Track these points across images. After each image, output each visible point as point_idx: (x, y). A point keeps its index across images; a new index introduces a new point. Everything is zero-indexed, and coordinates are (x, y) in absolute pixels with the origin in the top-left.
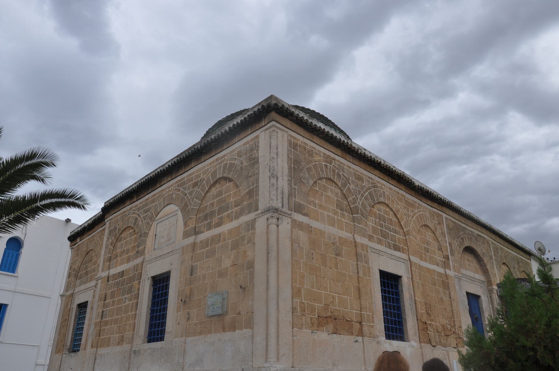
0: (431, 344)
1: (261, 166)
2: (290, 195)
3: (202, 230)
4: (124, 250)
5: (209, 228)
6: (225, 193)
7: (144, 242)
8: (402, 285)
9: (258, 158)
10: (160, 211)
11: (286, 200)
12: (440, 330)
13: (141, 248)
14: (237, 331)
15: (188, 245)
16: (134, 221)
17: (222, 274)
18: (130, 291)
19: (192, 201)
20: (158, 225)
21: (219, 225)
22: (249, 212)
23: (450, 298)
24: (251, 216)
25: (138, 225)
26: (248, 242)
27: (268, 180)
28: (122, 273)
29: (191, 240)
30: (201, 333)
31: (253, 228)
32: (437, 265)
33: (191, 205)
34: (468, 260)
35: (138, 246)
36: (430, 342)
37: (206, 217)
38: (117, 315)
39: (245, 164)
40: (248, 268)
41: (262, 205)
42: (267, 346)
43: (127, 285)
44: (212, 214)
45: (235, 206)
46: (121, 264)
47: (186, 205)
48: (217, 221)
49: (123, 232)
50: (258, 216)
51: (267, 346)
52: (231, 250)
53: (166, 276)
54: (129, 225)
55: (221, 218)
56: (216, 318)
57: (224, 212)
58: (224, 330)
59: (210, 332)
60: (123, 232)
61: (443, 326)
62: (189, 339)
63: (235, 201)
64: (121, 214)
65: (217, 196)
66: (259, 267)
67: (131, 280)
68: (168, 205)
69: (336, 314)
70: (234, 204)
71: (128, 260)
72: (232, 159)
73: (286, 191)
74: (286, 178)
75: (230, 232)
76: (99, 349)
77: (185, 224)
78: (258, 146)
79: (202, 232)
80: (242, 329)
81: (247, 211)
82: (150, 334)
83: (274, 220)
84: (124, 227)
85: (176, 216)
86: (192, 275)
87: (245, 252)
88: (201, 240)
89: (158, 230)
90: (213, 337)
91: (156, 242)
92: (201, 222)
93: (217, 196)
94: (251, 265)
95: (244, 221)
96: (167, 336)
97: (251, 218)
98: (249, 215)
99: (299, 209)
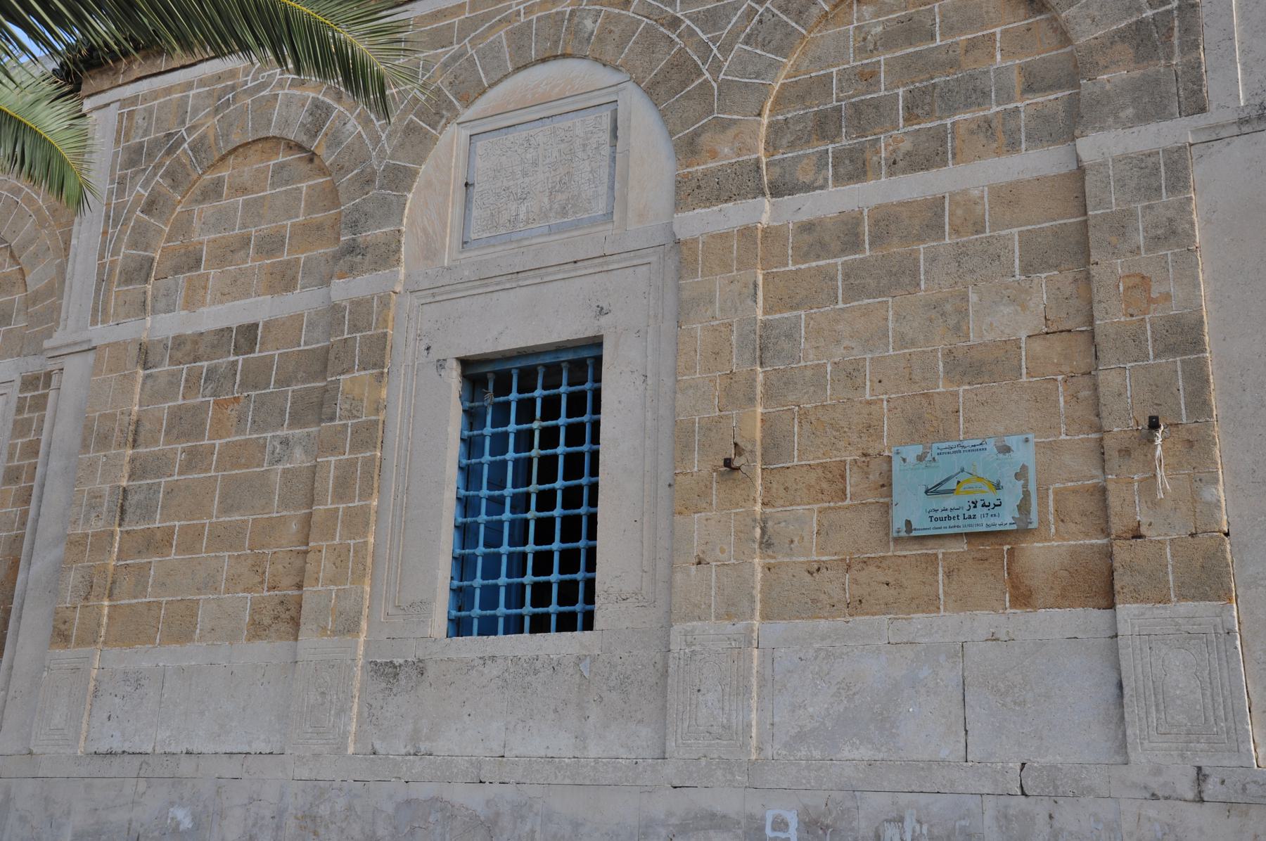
3: (803, 178)
4: (246, 242)
5: (855, 168)
6: (949, 29)
7: (391, 210)
10: (491, 86)
13: (374, 234)
15: (724, 237)
16: (303, 116)
17: (970, 367)
18: (318, 407)
20: (480, 144)
21: (927, 157)
22: (1143, 117)
24: (1175, 131)
25: (334, 140)
26: (1156, 241)
28: (248, 335)
30: (857, 605)
31: (1178, 180)
33: (716, 68)
35: (354, 226)
37: (824, 126)
38: (226, 509)
40: (1171, 350)
43: (284, 381)
44: (866, 116)
45: (1029, 89)
46: (224, 296)
47: (683, 69)
48: (906, 146)
49: (223, 158)
50: (1215, 137)
52: (1027, 269)
53: (548, 359)
54: (272, 132)
55: (940, 136)
56: (962, 546)
57: (952, 110)
59: (931, 604)
60: (223, 158)
63: (1022, 68)
64: (202, 83)
65: (888, 41)
67: (322, 362)
68: (543, 61)
70: (1017, 81)
71: (283, 280)
77: (688, 148)
79: (808, 188)
80: (1165, 600)
81: (1130, 111)
84: (236, 139)
85: (612, 106)
88: (804, 217)
89: (479, 163)
90: (944, 625)
92: (792, 146)
93: (888, 41)
95: (1118, 151)
96: (603, 610)
97: (1168, 143)
98: (1153, 127)
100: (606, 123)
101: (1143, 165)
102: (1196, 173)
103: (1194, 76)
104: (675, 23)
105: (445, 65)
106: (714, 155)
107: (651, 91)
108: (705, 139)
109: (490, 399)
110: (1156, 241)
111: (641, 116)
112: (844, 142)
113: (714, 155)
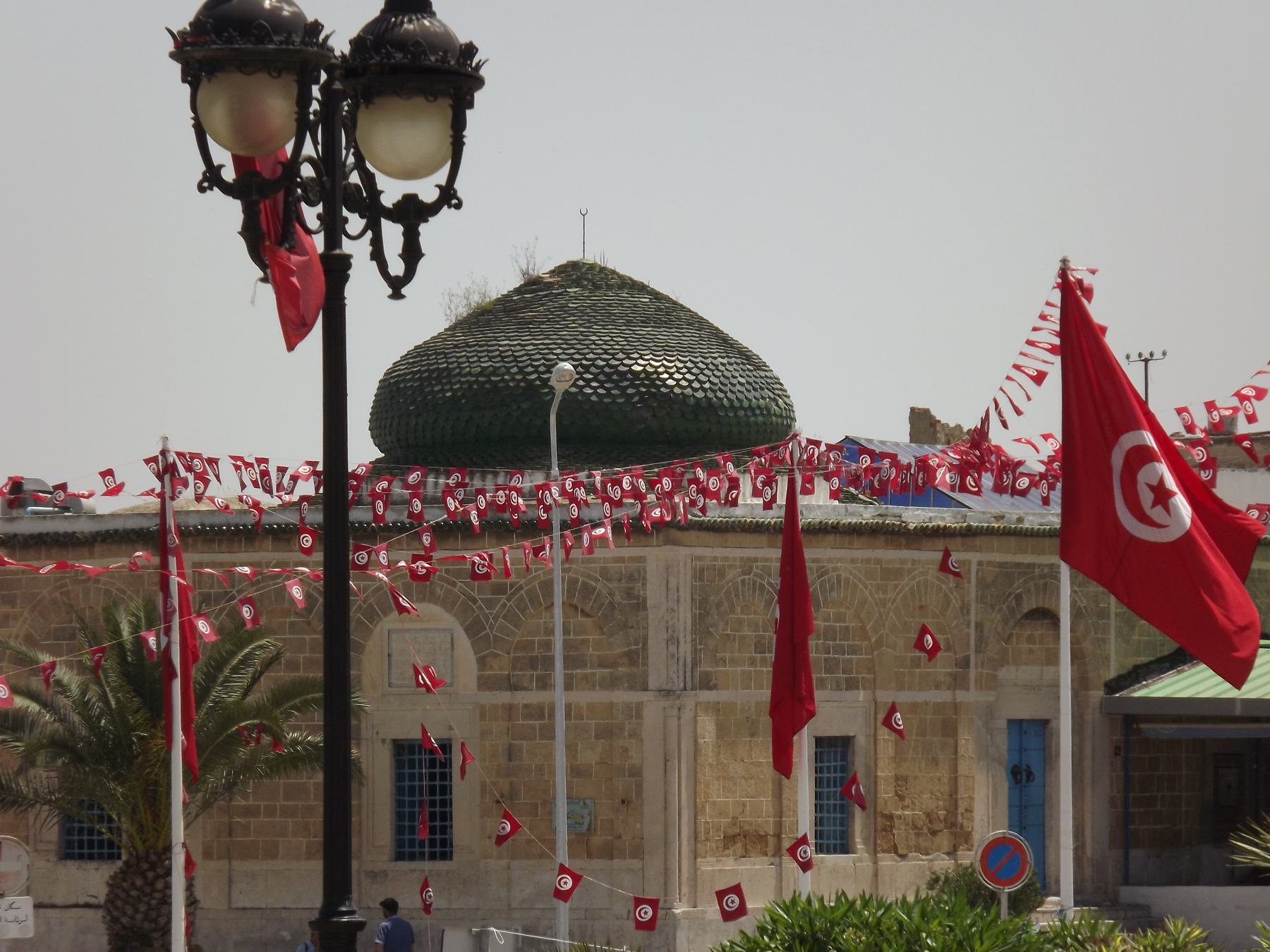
0: (896, 852)
1: (652, 617)
2: (694, 665)
8: (853, 752)
9: (645, 599)
11: (689, 674)
12: (920, 824)
14: (616, 861)
19: (495, 619)
23: (956, 752)
26: (630, 736)
27: (664, 643)
29: (504, 697)
32: (937, 687)
34: (1031, 639)
36: (895, 849)
39: (618, 598)
41: (653, 683)
42: (666, 883)
51: (666, 883)
52: (597, 737)
58: (590, 856)
61: (928, 815)
62: (516, 864)
66: (651, 776)
69: (746, 827)
72: (589, 577)
73: (689, 660)
74: (689, 639)
75: (592, 707)
76: (233, 862)
77: (482, 662)
78: (645, 579)
79: (526, 689)
82: (399, 844)
83: (675, 712)
86: (510, 760)
87: (625, 750)
91: (394, 670)
92: (521, 669)
94: (636, 773)
99: (706, 683)
100: (449, 639)
101: (628, 706)
102: (645, 712)
103: (645, 675)
104: (475, 601)
105: (374, 591)
106: (491, 668)
107: (466, 630)
108: (488, 659)
109: (406, 758)
110: (630, 736)
111: (464, 641)
112: (539, 672)
113: (491, 668)
